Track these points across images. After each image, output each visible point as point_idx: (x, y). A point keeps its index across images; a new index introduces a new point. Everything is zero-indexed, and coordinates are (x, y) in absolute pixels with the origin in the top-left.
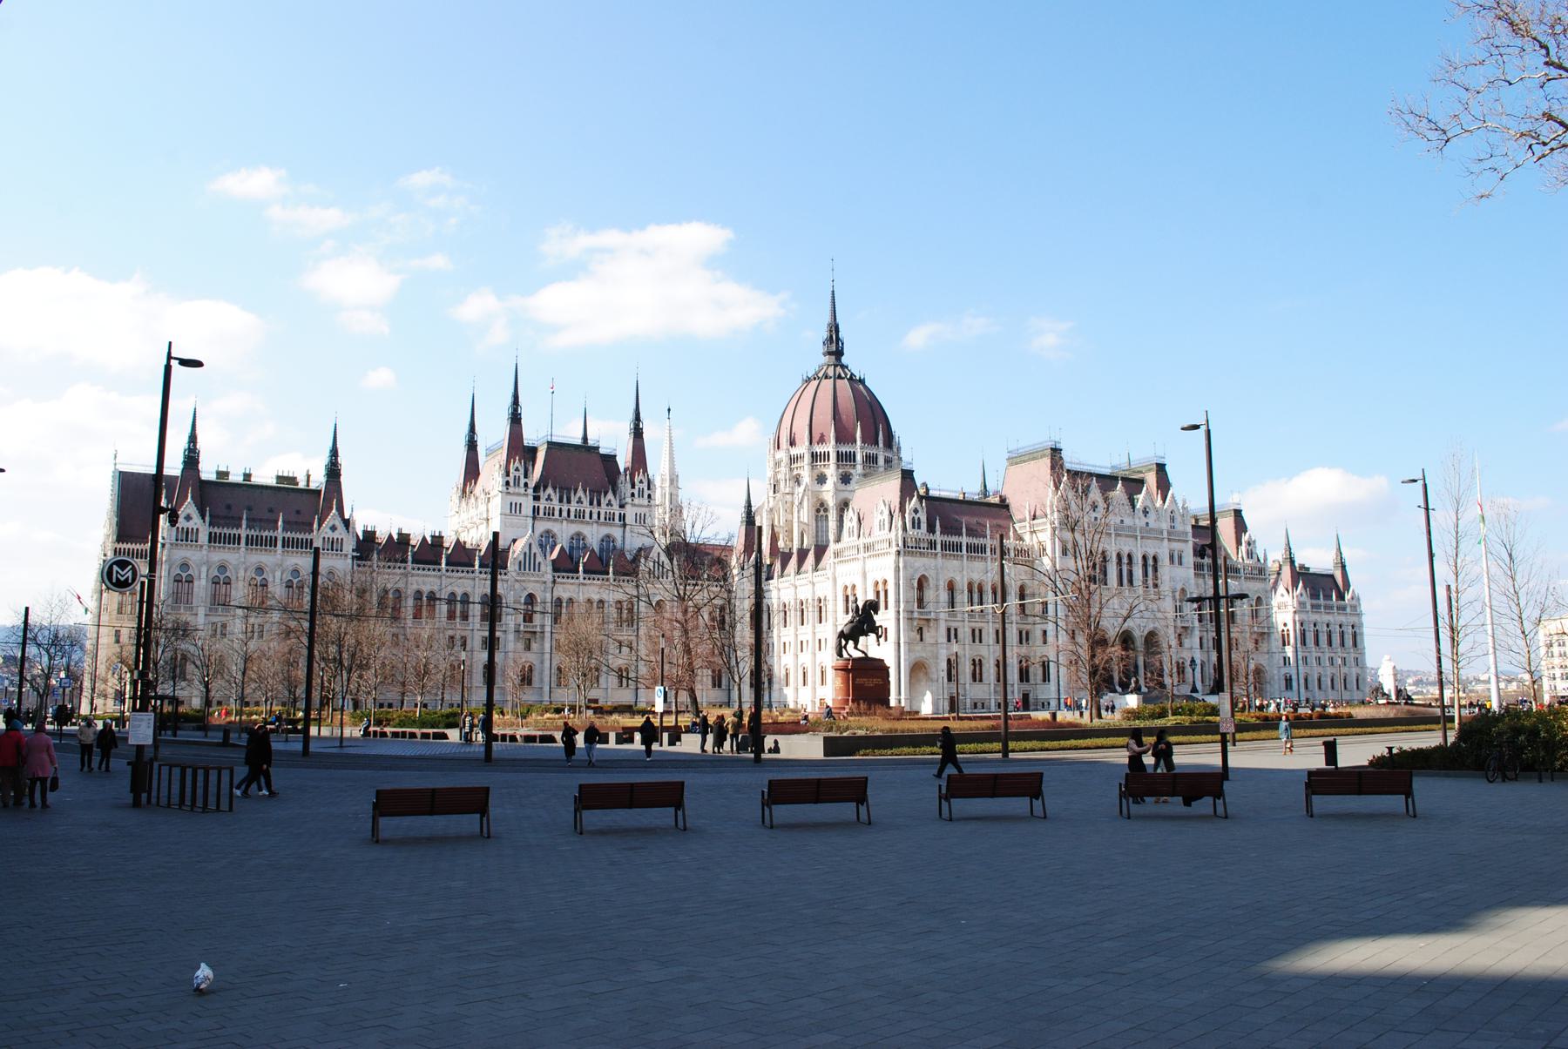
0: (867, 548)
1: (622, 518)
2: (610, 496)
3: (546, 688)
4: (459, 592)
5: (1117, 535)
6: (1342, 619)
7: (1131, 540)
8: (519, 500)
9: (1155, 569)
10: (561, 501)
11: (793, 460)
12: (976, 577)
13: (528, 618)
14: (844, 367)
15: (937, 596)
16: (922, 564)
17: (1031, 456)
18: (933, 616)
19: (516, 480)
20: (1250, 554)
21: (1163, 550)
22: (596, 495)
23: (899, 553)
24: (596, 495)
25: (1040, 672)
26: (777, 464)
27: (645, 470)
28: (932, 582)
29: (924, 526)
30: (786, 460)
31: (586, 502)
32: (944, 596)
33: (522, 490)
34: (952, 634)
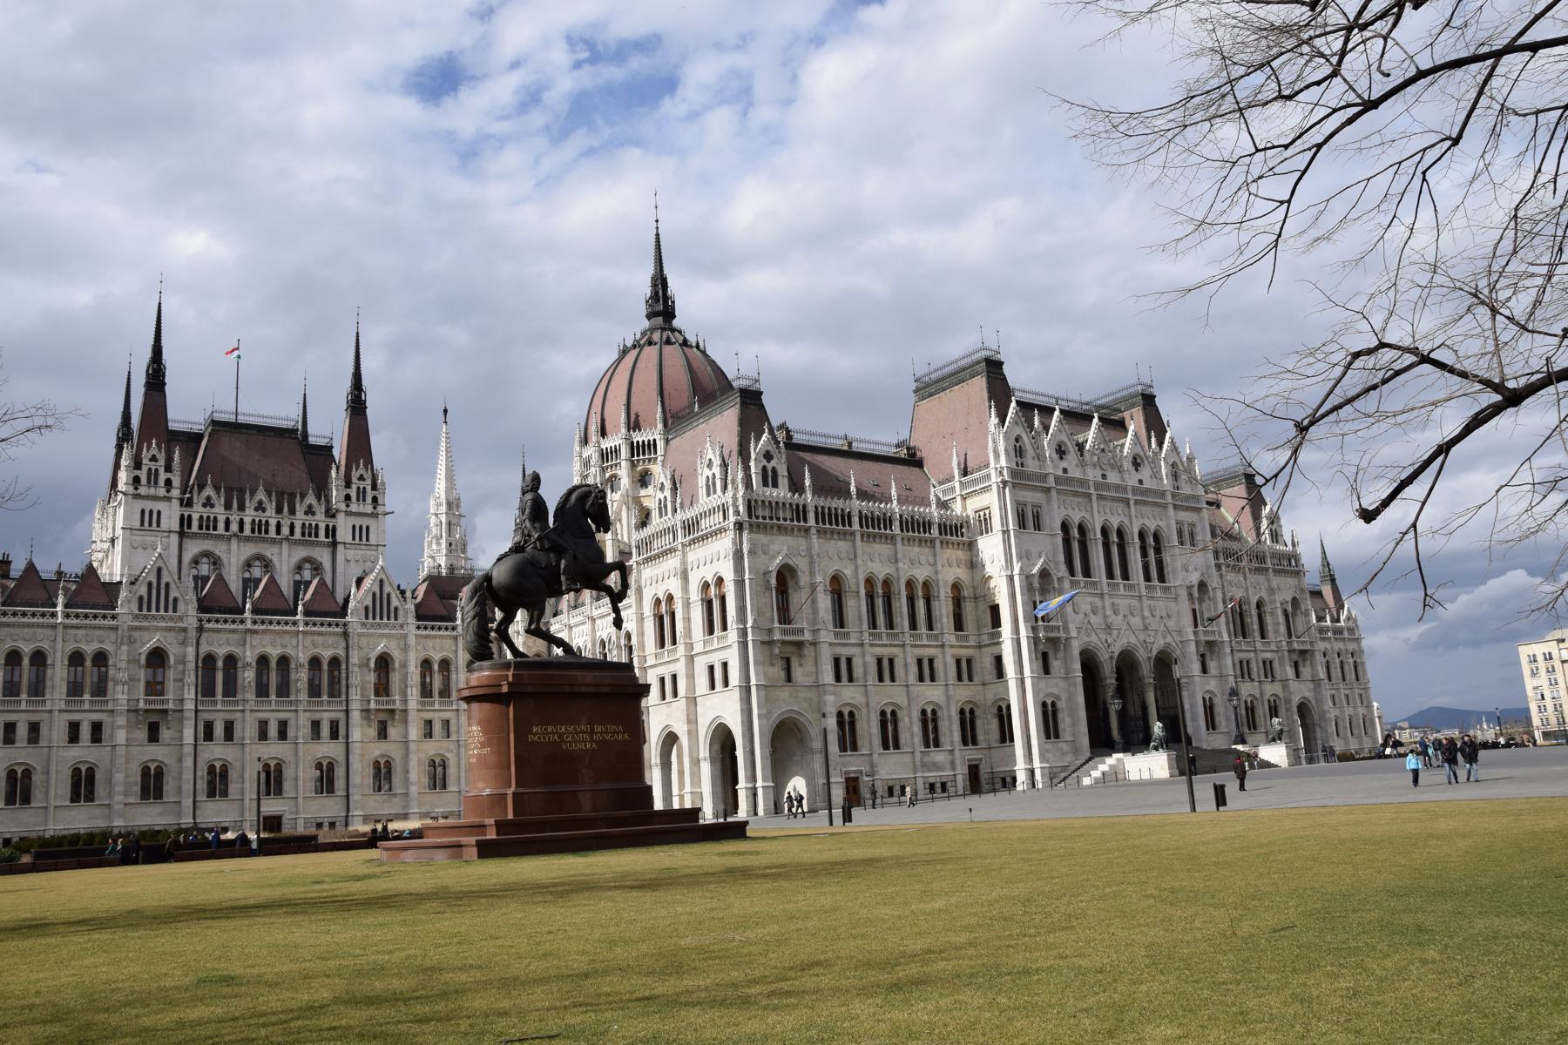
0: (690, 526)
1: (331, 532)
2: (311, 499)
4: (27, 649)
5: (1100, 497)
6: (1338, 646)
7: (1120, 507)
8: (156, 506)
9: (1158, 550)
10: (228, 506)
11: (605, 455)
12: (881, 570)
13: (155, 688)
14: (673, 330)
16: (781, 549)
17: (955, 377)
18: (807, 636)
19: (153, 477)
20: (1275, 536)
21: (1167, 522)
22: (286, 499)
23: (739, 526)
24: (286, 499)
25: (995, 724)
26: (586, 464)
28: (804, 579)
29: (783, 482)
30: (595, 457)
31: (271, 510)
32: (825, 603)
33: (162, 492)
34: (843, 669)
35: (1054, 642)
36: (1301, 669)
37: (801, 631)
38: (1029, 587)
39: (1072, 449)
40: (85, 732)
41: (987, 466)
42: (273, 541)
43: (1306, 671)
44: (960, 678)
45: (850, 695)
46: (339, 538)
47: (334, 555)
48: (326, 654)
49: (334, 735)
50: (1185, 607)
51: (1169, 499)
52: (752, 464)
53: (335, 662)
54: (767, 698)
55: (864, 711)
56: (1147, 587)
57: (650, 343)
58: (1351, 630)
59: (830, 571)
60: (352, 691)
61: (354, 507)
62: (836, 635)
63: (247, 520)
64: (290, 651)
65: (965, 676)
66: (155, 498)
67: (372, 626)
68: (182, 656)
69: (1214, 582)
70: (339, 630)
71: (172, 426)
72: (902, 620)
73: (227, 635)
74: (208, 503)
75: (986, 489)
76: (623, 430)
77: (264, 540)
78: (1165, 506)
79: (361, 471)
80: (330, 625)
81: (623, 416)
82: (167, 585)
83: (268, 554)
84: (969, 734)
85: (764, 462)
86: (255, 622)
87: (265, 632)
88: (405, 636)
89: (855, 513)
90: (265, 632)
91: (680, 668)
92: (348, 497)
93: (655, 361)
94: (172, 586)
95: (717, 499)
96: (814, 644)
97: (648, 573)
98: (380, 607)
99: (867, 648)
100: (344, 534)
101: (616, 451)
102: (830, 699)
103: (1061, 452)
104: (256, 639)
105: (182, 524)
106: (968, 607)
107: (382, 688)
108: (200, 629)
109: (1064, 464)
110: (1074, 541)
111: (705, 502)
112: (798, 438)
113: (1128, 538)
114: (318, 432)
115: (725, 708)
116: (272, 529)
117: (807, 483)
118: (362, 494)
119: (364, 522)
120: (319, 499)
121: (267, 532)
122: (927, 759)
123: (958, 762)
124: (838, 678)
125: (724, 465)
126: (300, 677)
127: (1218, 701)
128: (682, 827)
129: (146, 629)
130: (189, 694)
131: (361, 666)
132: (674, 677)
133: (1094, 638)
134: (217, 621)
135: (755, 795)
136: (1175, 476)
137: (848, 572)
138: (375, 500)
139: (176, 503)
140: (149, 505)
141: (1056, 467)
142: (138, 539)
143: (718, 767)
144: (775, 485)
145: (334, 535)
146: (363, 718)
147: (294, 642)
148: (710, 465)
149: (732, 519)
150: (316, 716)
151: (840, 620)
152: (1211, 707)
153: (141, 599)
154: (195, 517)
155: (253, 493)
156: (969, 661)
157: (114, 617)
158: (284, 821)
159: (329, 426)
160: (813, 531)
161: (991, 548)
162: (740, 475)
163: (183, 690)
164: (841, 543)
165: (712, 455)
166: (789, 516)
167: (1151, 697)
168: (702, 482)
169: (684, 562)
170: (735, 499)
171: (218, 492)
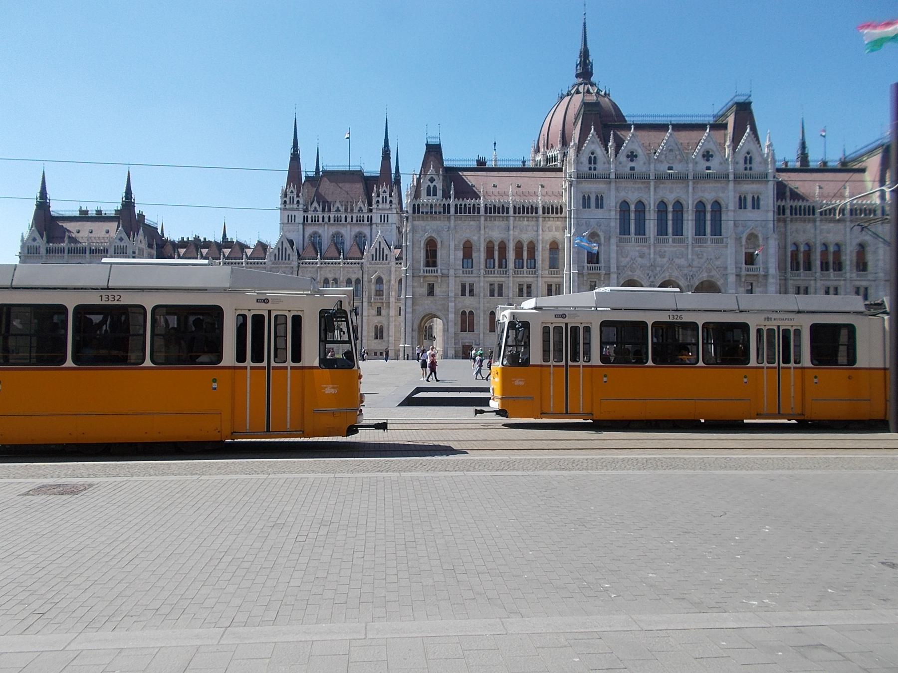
1: (370, 219)
8: (293, 213)
29: (440, 193)
33: (295, 206)
34: (467, 290)
46: (373, 222)
57: (578, 92)
63: (332, 216)
66: (293, 209)
72: (511, 265)
83: (320, 232)
100: (376, 219)
102: (452, 305)
107: (379, 293)
108: (299, 266)
109: (633, 164)
140: (290, 213)
144: (435, 194)
154: (310, 216)
164: (472, 223)
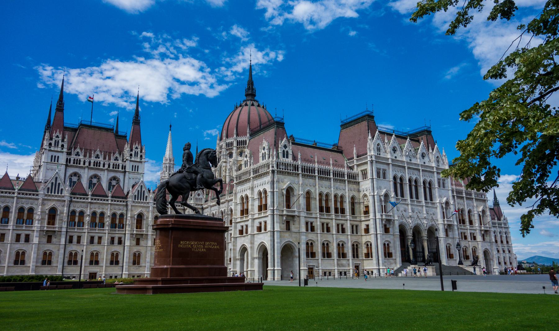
0: (256, 171)
1: (124, 167)
2: (117, 155)
3: (60, 266)
5: (409, 168)
7: (416, 172)
12: (325, 191)
15: (299, 202)
17: (357, 121)
18: (296, 214)
19: (57, 143)
22: (107, 154)
24: (107, 154)
27: (140, 142)
28: (296, 193)
29: (290, 157)
32: (302, 201)
35: (389, 221)
36: (485, 237)
37: (294, 211)
38: (381, 200)
39: (398, 149)
40: (23, 238)
41: (366, 154)
42: (102, 170)
43: (487, 238)
44: (353, 233)
45: (312, 236)
47: (125, 176)
48: (119, 212)
49: (120, 242)
50: (439, 211)
51: (435, 170)
52: (279, 149)
53: (122, 215)
54: (281, 237)
55: (316, 243)
56: (425, 202)
57: (246, 105)
58: (505, 224)
59: (306, 190)
60: (127, 226)
61: (133, 159)
62: (307, 213)
63: (92, 162)
64: (105, 211)
65: (355, 232)
67: (137, 202)
68: (63, 211)
69: (452, 202)
70: (125, 203)
71: (65, 125)
73: (81, 204)
74: (78, 154)
75: (366, 163)
76: (235, 136)
77: (99, 169)
78: (433, 172)
79: (137, 145)
80: (121, 202)
81: (235, 131)
82: (59, 184)
84: (355, 254)
85: (284, 149)
86: (92, 199)
87: (96, 203)
88: (149, 207)
89: (316, 169)
90: (96, 203)
91: (249, 223)
92: (131, 155)
93: (248, 111)
94: (61, 184)
95: (265, 162)
96: (299, 217)
97: (239, 188)
98: (141, 196)
99: (318, 219)
101: (232, 144)
103: (394, 150)
104: (92, 206)
105: (67, 162)
106: (356, 206)
108: (71, 201)
110: (398, 183)
111: (261, 162)
112: (297, 141)
113: (419, 184)
114: (122, 130)
115: (265, 239)
116: (102, 165)
117: (299, 157)
118: (136, 154)
119: (137, 164)
120: (120, 155)
121: (99, 166)
122: (339, 262)
123: (351, 264)
124: (307, 230)
125: (269, 149)
126: (107, 221)
127: (452, 247)
128: (238, 284)
129: (50, 200)
130: (65, 225)
131: (131, 217)
132: (247, 226)
133: (404, 220)
134: (78, 198)
135: (274, 272)
136: (438, 161)
137: (313, 191)
138: (141, 156)
139: (65, 154)
140: (54, 154)
141: (392, 156)
142: (49, 166)
143: (261, 261)
144: (287, 157)
145: (125, 169)
146: (131, 237)
147: (107, 207)
148: (264, 149)
149: (271, 169)
150: (113, 236)
151: (308, 208)
152: (449, 249)
153: (48, 188)
154: (72, 159)
155: (95, 151)
156: (357, 226)
157: (37, 195)
158: (98, 275)
159: (126, 129)
160: (300, 175)
161: (366, 185)
162: (275, 153)
163: (61, 223)
164: (310, 180)
165: (265, 144)
166: (292, 169)
167: (425, 244)
168: (261, 155)
169: (253, 184)
170: (272, 161)
171: (81, 151)
